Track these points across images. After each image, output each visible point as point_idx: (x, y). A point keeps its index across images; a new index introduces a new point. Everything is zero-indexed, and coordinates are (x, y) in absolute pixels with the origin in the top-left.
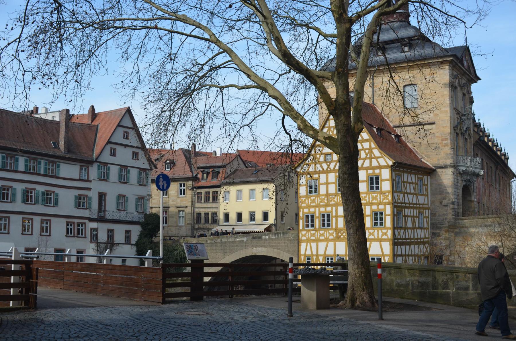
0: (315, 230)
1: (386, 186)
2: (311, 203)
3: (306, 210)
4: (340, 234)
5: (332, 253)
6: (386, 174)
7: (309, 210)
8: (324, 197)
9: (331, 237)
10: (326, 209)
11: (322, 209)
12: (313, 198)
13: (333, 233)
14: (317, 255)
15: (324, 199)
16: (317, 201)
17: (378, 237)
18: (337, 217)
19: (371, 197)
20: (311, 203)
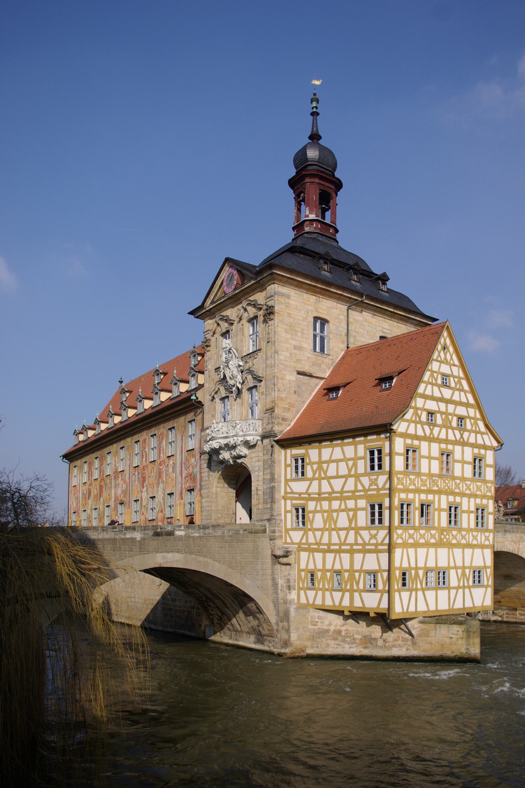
0: (414, 528)
1: (490, 474)
2: (410, 484)
3: (403, 496)
4: (443, 537)
5: (434, 565)
6: (490, 457)
7: (407, 496)
8: (425, 478)
9: (433, 541)
10: (427, 497)
11: (423, 496)
12: (412, 477)
13: (435, 534)
14: (417, 568)
15: (426, 481)
16: (418, 483)
17: (481, 541)
18: (440, 510)
19: (475, 486)
20: (410, 484)
